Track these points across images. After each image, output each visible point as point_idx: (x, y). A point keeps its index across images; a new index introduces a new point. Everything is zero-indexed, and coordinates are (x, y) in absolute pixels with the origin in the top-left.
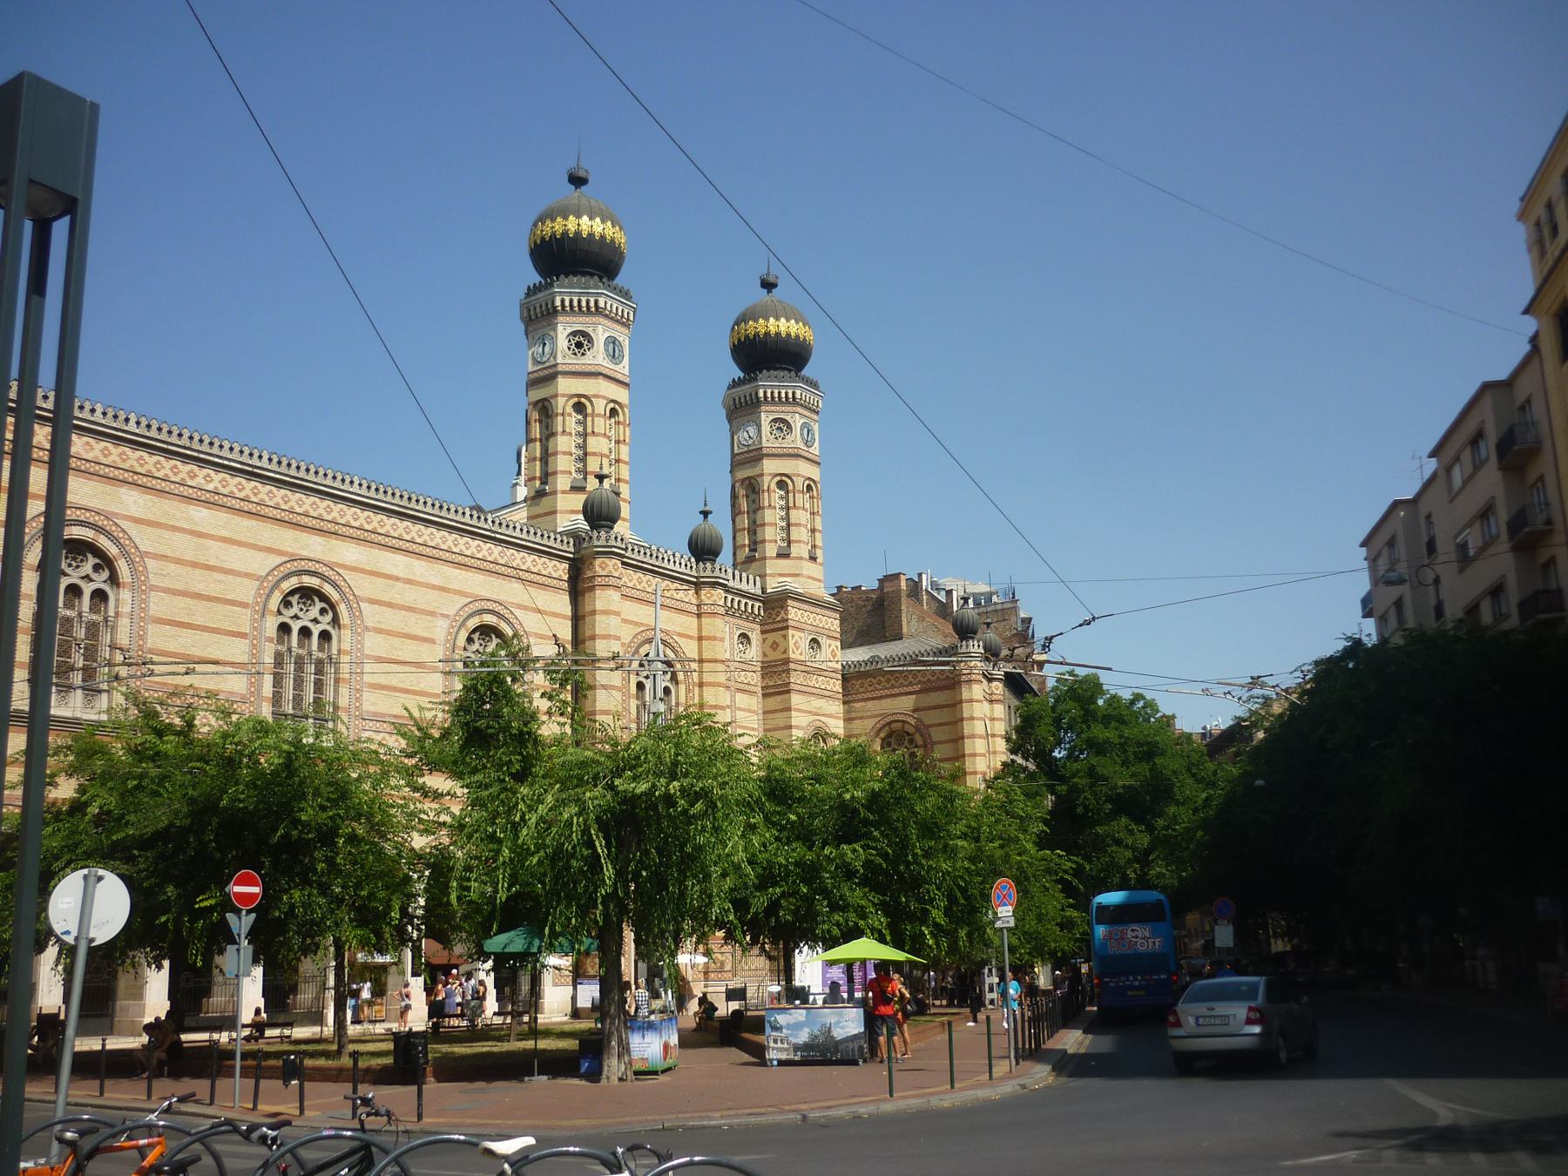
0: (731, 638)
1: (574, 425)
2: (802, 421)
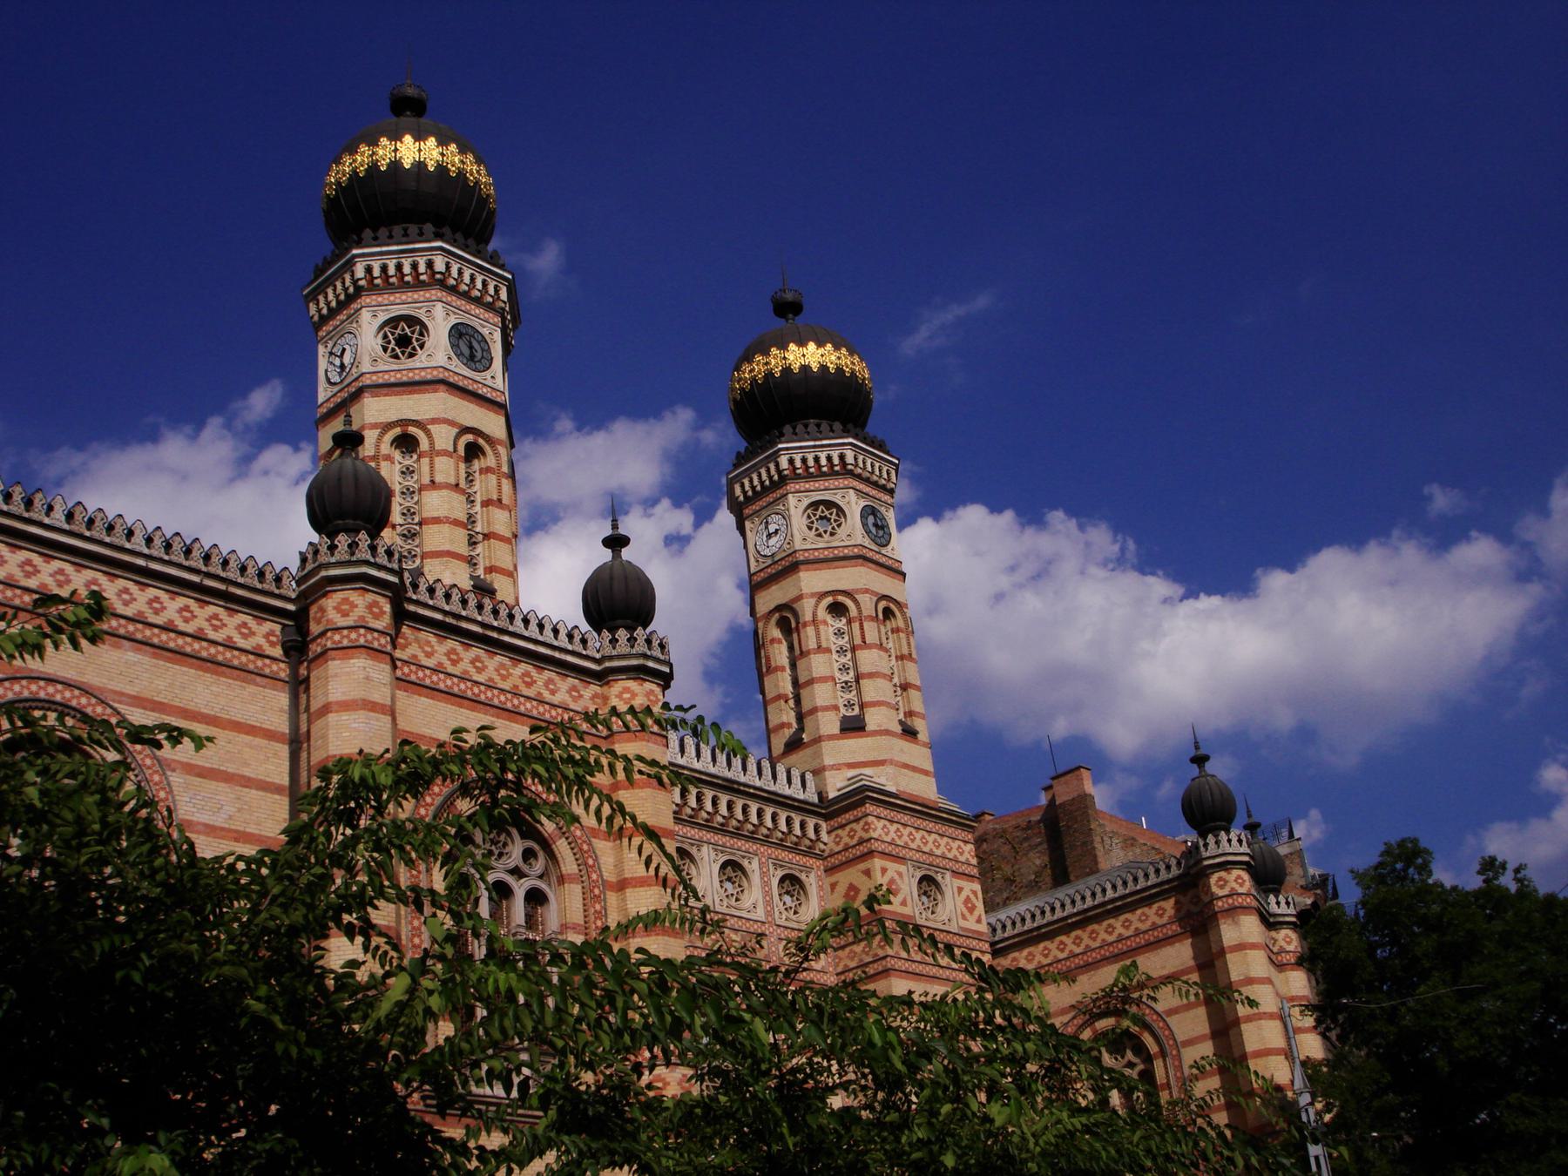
0: (766, 884)
1: (398, 478)
2: (863, 503)
